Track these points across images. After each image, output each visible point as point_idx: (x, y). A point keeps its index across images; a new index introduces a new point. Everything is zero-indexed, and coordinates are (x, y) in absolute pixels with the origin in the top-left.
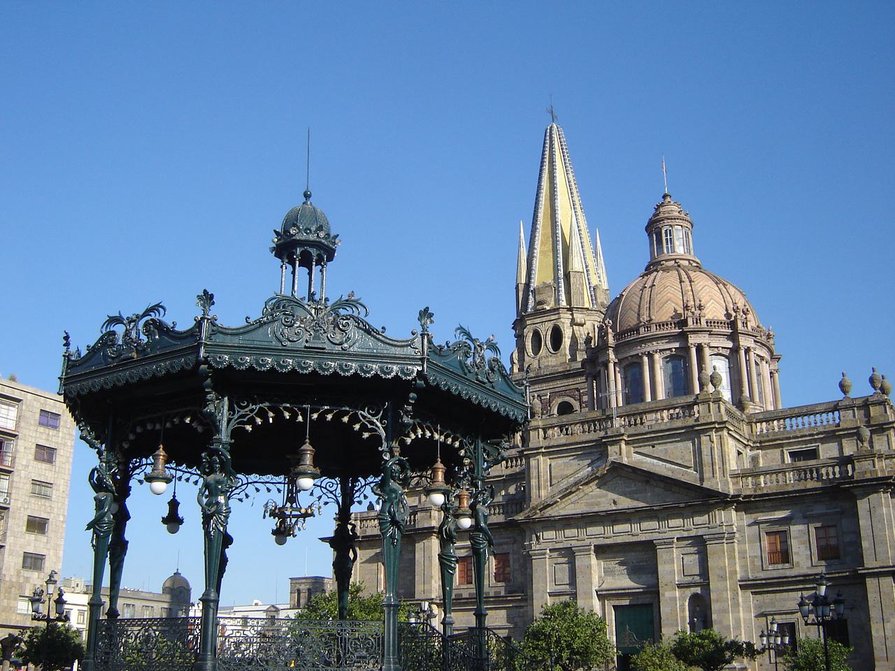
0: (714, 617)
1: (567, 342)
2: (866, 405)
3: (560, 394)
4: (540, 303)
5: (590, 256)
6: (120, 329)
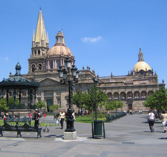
0: (61, 101)
1: (41, 53)
2: (86, 71)
3: (39, 62)
4: (37, 45)
5: (46, 37)
6: (5, 80)
